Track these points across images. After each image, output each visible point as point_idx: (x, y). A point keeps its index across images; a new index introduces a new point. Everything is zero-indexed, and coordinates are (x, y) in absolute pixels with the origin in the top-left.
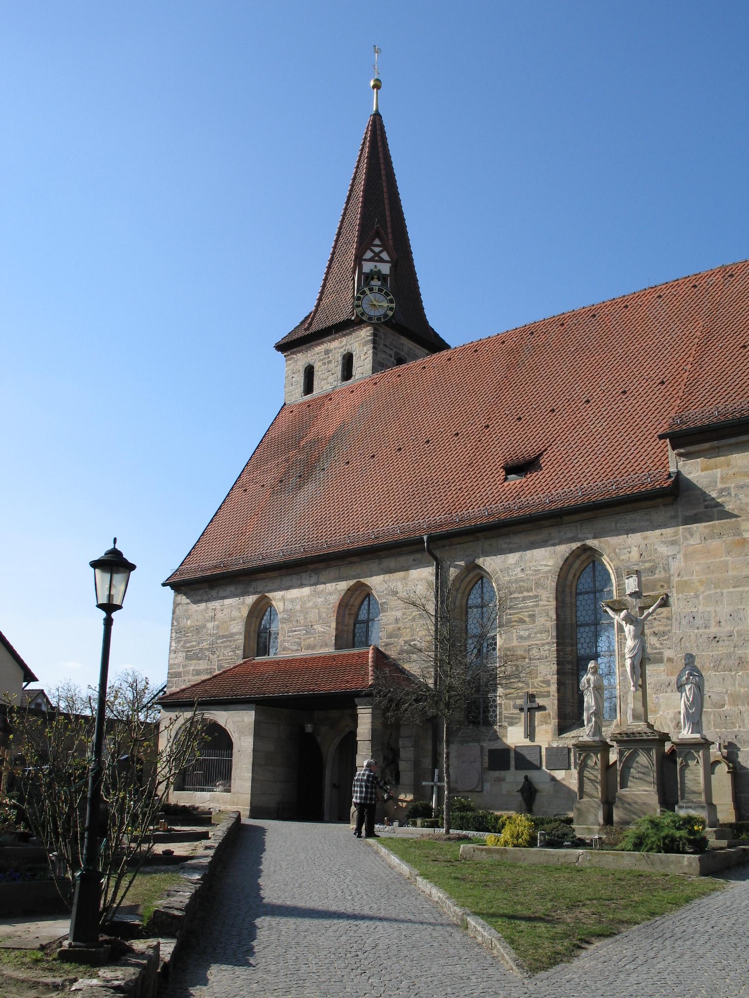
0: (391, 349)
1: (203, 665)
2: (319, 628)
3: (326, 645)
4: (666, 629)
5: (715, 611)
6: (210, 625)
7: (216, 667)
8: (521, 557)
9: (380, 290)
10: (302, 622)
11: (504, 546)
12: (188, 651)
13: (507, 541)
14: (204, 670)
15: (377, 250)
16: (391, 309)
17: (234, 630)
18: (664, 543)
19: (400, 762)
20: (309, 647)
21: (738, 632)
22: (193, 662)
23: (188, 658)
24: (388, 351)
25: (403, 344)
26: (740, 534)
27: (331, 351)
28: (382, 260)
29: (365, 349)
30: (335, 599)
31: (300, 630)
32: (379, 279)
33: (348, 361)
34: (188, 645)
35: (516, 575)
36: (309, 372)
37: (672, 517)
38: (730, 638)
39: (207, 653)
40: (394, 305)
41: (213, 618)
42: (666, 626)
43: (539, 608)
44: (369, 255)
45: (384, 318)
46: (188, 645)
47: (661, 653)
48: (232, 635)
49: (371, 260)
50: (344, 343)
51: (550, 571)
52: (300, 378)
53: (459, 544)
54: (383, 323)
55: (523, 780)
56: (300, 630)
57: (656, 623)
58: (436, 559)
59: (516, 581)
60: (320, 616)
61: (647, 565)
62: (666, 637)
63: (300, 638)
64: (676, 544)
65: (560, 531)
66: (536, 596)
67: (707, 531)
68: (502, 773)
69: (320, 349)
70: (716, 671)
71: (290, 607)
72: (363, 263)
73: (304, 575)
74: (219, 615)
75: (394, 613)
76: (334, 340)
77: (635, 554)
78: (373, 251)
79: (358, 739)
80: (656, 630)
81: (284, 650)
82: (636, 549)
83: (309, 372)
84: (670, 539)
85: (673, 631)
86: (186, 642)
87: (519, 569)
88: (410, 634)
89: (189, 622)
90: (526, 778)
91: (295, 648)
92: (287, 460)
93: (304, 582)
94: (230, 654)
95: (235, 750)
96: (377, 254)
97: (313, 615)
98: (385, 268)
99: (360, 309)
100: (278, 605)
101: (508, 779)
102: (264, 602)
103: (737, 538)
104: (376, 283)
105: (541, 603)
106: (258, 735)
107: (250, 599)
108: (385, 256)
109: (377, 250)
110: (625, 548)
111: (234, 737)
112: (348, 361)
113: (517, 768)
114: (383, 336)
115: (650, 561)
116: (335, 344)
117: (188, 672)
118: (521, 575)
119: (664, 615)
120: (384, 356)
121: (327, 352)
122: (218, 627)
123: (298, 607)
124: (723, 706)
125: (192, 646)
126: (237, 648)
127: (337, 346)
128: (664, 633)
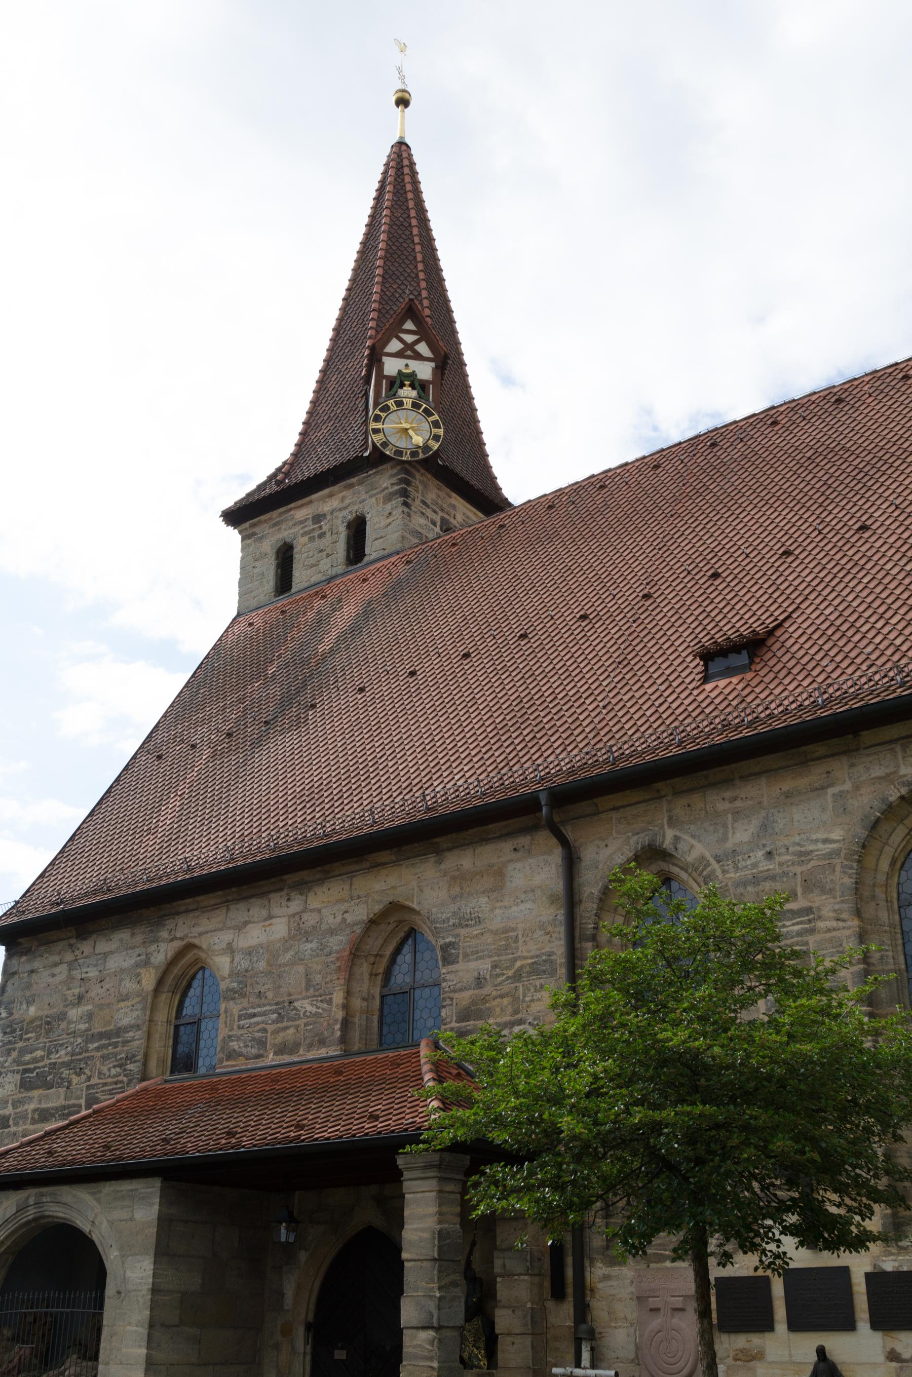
0: (435, 512)
1: (55, 1099)
2: (306, 1006)
3: (322, 1042)
6: (74, 1013)
7: (83, 1102)
8: (764, 827)
9: (416, 406)
10: (270, 995)
11: (722, 806)
12: (26, 1071)
13: (728, 794)
14: (57, 1109)
15: (410, 338)
16: (436, 438)
17: (125, 1022)
19: (498, 1313)
20: (281, 1050)
22: (36, 1093)
23: (26, 1085)
24: (429, 513)
25: (454, 507)
27: (324, 516)
28: (418, 356)
29: (388, 507)
30: (339, 943)
31: (264, 1014)
32: (413, 386)
33: (357, 530)
34: (28, 1057)
35: (755, 865)
36: (285, 557)
39: (66, 1073)
40: (441, 432)
41: (80, 998)
43: (817, 937)
44: (395, 346)
45: (431, 415)
46: (28, 1057)
48: (119, 1032)
49: (399, 355)
50: (347, 502)
51: (837, 853)
52: (269, 568)
53: (615, 809)
54: (418, 462)
55: (814, 1358)
56: (264, 1014)
58: (564, 842)
59: (756, 880)
60: (309, 981)
63: (265, 1030)
65: (852, 765)
66: (809, 910)
68: (755, 1340)
69: (302, 512)
71: (245, 964)
72: (385, 359)
73: (275, 897)
74: (96, 991)
75: (473, 965)
76: (331, 495)
78: (402, 341)
79: (405, 1255)
81: (229, 1057)
83: (285, 557)
86: (23, 1051)
87: (760, 854)
88: (510, 1010)
89: (32, 1010)
90: (821, 1352)
91: (254, 1051)
92: (240, 701)
93: (276, 911)
94: (113, 1072)
95: (110, 1291)
96: (410, 347)
97: (294, 979)
98: (424, 371)
99: (381, 436)
100: (222, 964)
101: (771, 1355)
102: (189, 957)
104: (408, 393)
105: (821, 925)
106: (163, 1253)
107: (162, 953)
108: (423, 348)
109: (410, 338)
111: (111, 1257)
112: (357, 530)
113: (795, 1325)
114: (420, 488)
116: (334, 503)
117: (23, 1117)
118: (764, 866)
120: (422, 521)
121: (318, 518)
122: (90, 1016)
123: (262, 965)
125: (35, 1060)
126: (130, 1058)
127: (336, 506)
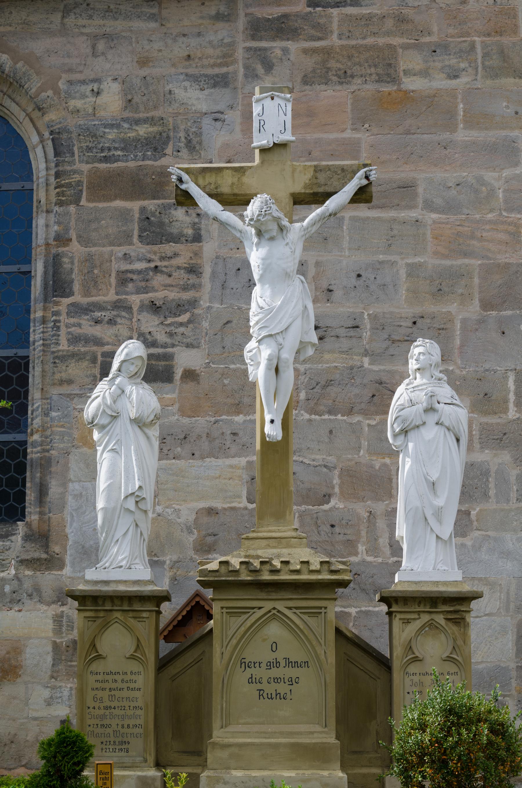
4: (186, 296)
5: (318, 264)
18: (195, 79)
21: (374, 318)
26: (394, 80)
37: (219, 17)
38: (352, 333)
42: (185, 288)
47: (169, 357)
57: (159, 280)
61: (143, 130)
62: (184, 318)
64: (226, 85)
67: (310, 63)
70: (312, 411)
77: (111, 101)
80: (158, 296)
82: (116, 87)
84: (210, 71)
85: (204, 303)
103: (386, 88)
110: (83, 82)
115: (150, 121)
119: (180, 261)
124: (327, 498)
128: (179, 307)
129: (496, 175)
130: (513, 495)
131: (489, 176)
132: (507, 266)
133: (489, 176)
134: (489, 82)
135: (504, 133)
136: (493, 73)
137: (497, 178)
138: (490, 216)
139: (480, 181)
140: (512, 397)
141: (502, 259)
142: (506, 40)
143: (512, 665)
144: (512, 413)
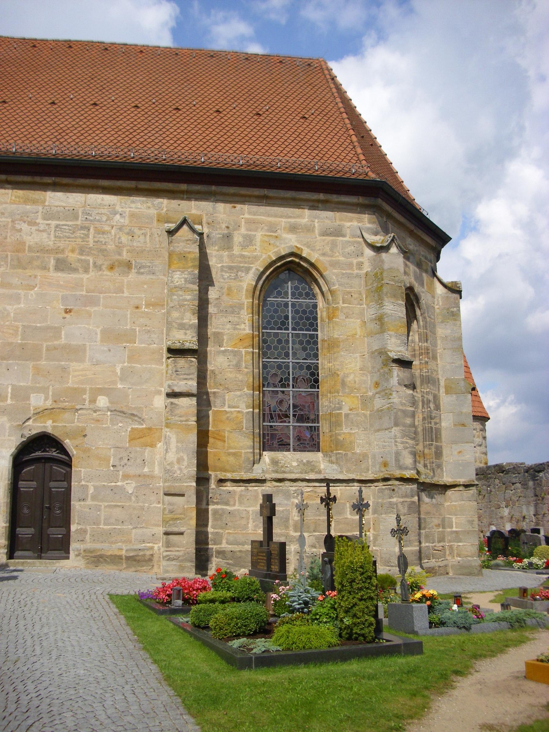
129: (11, 307)
130: (7, 434)
131: (9, 308)
132: (12, 343)
133: (9, 308)
134: (12, 270)
135: (16, 291)
136: (13, 267)
137: (11, 308)
138: (7, 323)
139: (5, 309)
140: (9, 395)
141: (10, 340)
142: (20, 255)
143: (2, 501)
144: (9, 401)
